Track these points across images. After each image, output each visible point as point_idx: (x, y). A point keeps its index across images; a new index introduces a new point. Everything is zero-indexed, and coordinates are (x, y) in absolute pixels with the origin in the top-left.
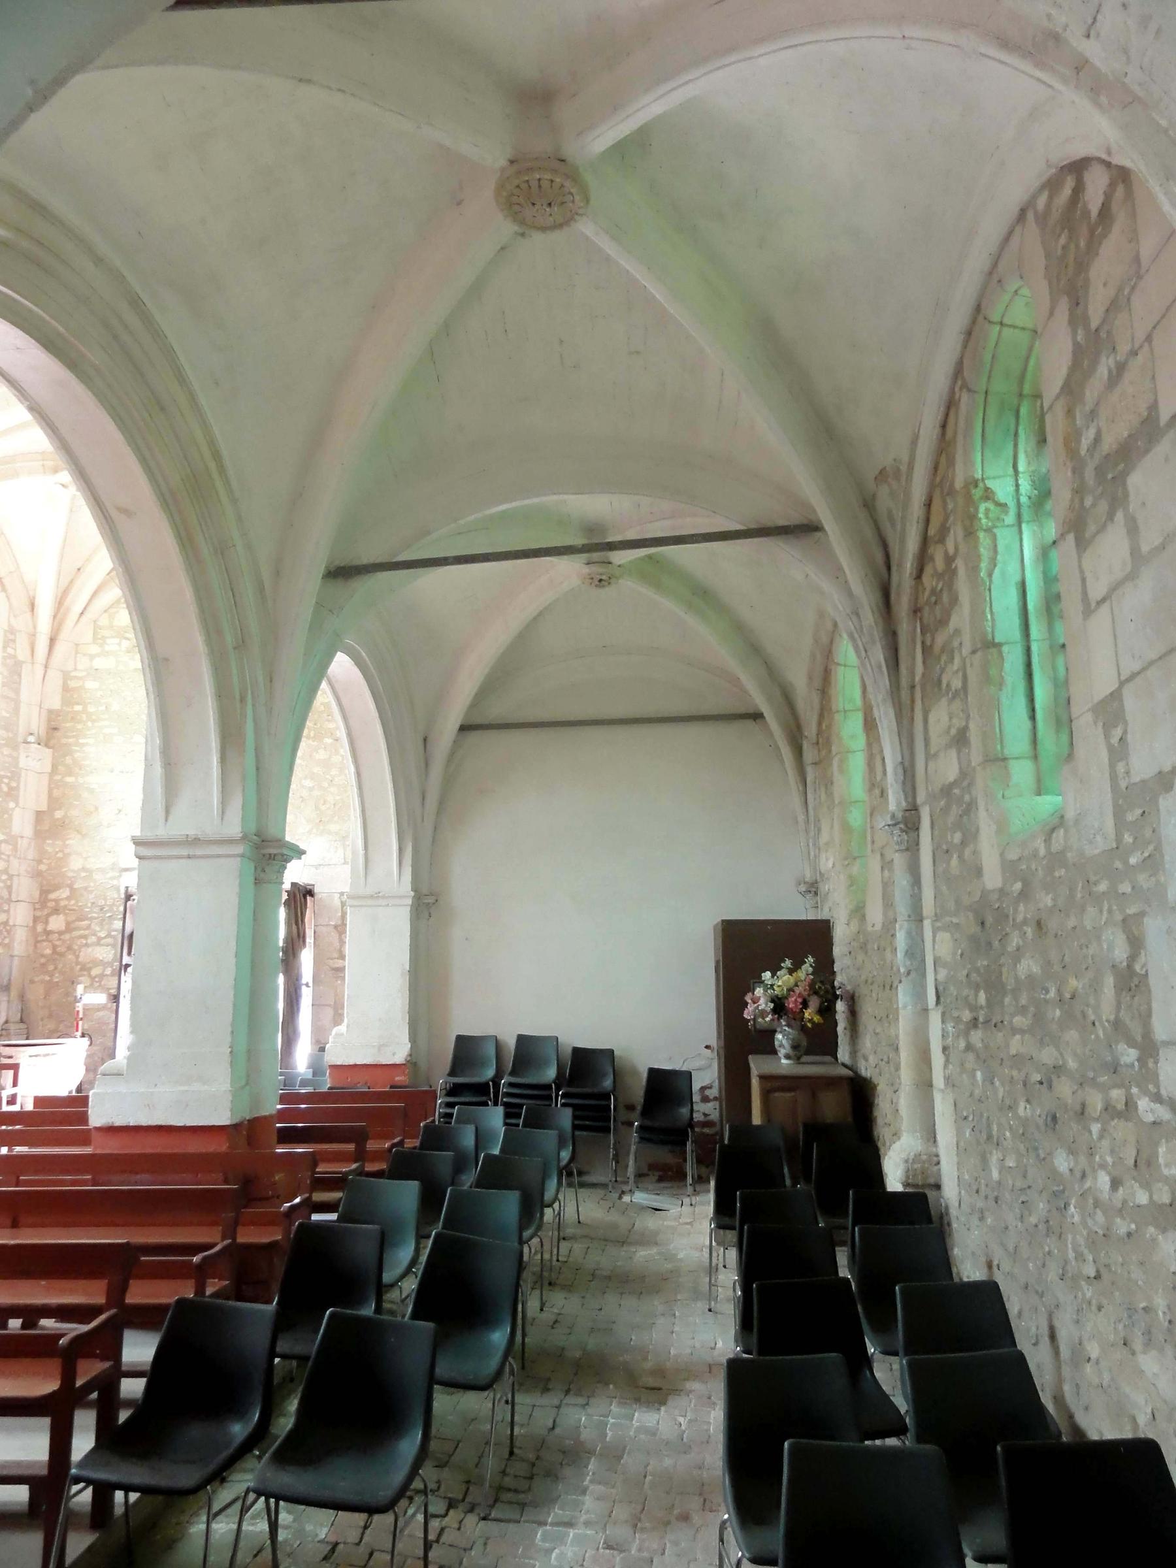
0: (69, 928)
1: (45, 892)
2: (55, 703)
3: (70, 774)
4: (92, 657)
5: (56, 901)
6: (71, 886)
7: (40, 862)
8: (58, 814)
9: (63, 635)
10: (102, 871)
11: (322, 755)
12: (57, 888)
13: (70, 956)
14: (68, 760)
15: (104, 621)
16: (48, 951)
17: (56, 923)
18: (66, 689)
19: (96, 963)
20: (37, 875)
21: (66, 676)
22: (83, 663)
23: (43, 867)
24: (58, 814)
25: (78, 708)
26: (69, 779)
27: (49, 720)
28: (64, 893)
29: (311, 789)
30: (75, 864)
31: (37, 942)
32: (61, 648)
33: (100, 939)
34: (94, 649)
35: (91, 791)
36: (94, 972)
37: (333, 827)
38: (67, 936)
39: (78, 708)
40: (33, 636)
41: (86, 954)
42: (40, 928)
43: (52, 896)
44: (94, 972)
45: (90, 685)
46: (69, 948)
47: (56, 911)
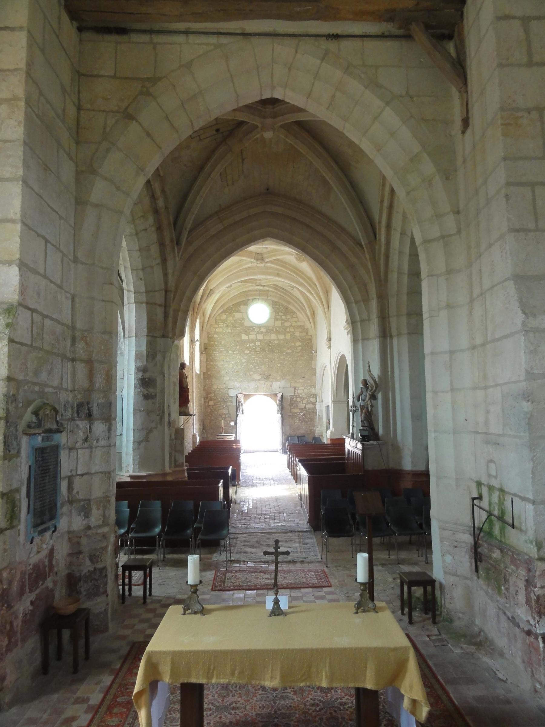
0: (215, 405)
1: (207, 394)
2: (206, 341)
3: (211, 361)
4: (216, 328)
5: (211, 397)
6: (214, 393)
7: (205, 386)
8: (209, 373)
9: (209, 322)
10: (223, 389)
11: (282, 357)
12: (211, 393)
13: (216, 412)
14: (211, 358)
15: (218, 318)
16: (209, 411)
17: (211, 403)
18: (208, 337)
19: (223, 414)
20: (204, 390)
21: (208, 333)
22: (213, 330)
23: (206, 388)
24: (209, 373)
25: (212, 343)
26: (212, 363)
27: (204, 346)
28: (213, 395)
29: (280, 367)
30: (215, 387)
31: (206, 408)
32: (209, 325)
33: (224, 408)
34: (216, 326)
35: (218, 367)
36: (223, 416)
37: (287, 377)
38: (214, 407)
39: (212, 343)
40: (203, 323)
41: (220, 412)
42: (206, 405)
43: (209, 396)
44: (223, 416)
45: (216, 336)
46: (215, 410)
47: (211, 400)
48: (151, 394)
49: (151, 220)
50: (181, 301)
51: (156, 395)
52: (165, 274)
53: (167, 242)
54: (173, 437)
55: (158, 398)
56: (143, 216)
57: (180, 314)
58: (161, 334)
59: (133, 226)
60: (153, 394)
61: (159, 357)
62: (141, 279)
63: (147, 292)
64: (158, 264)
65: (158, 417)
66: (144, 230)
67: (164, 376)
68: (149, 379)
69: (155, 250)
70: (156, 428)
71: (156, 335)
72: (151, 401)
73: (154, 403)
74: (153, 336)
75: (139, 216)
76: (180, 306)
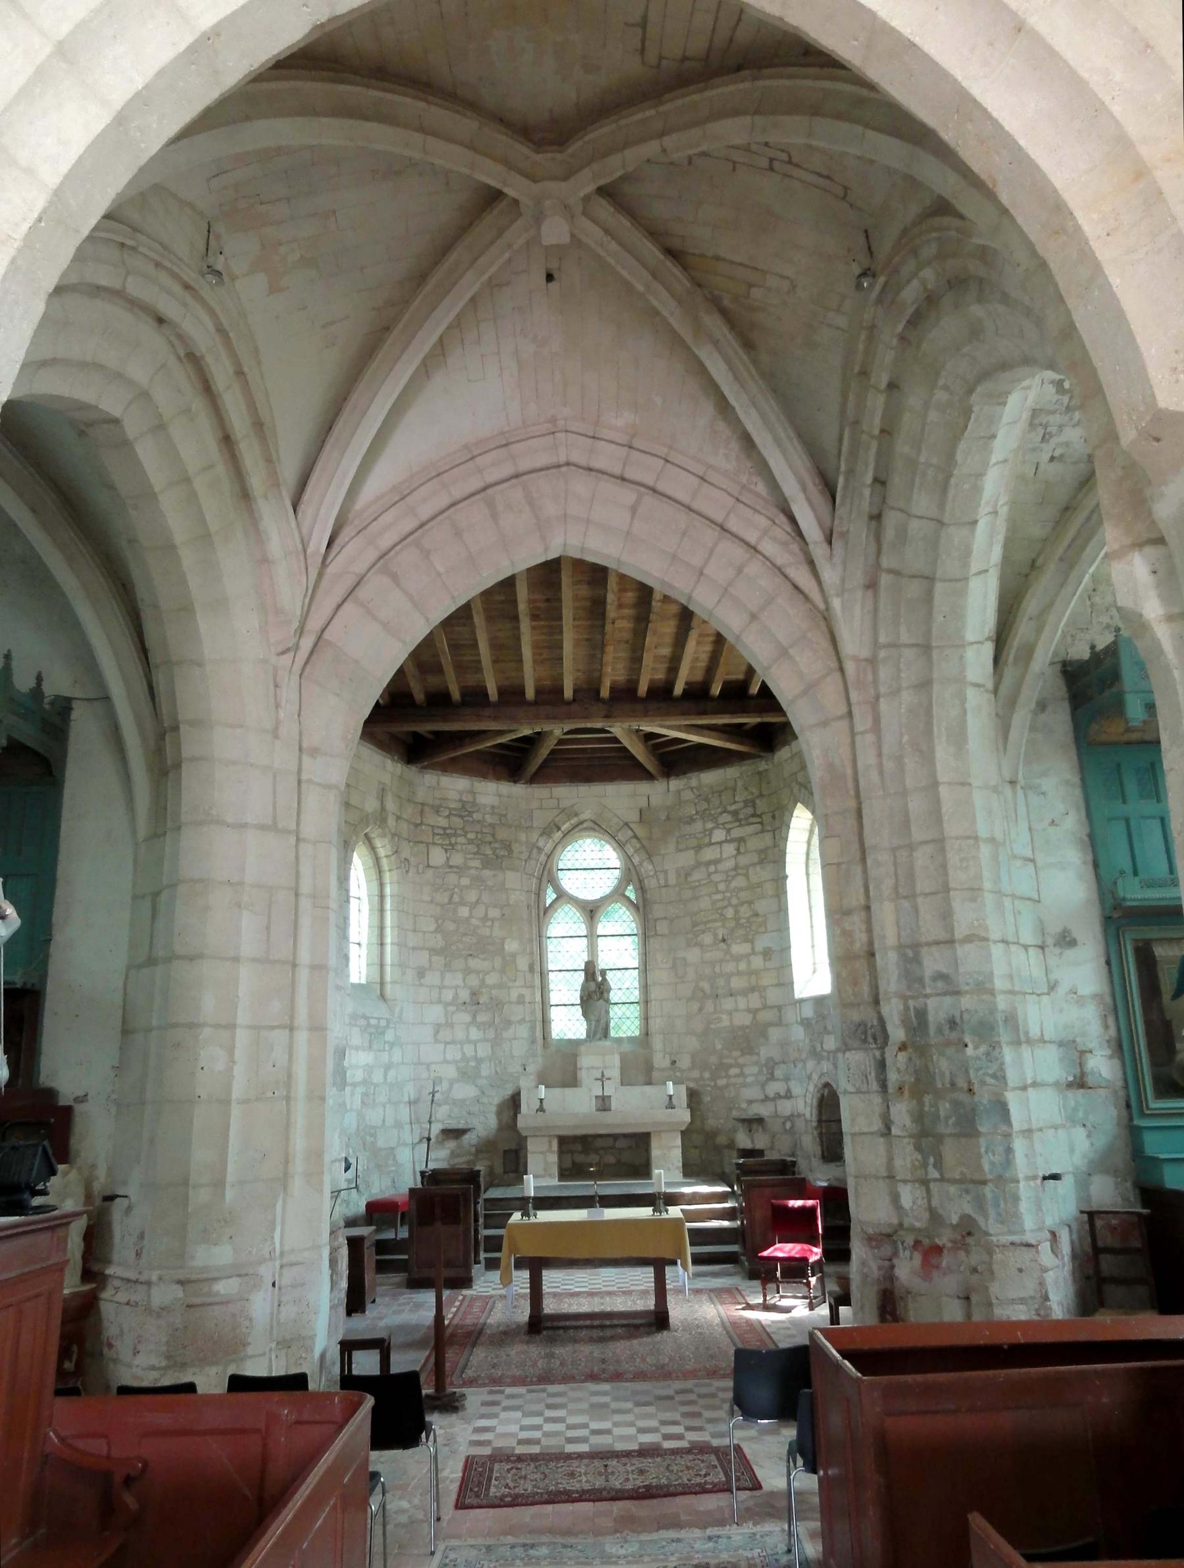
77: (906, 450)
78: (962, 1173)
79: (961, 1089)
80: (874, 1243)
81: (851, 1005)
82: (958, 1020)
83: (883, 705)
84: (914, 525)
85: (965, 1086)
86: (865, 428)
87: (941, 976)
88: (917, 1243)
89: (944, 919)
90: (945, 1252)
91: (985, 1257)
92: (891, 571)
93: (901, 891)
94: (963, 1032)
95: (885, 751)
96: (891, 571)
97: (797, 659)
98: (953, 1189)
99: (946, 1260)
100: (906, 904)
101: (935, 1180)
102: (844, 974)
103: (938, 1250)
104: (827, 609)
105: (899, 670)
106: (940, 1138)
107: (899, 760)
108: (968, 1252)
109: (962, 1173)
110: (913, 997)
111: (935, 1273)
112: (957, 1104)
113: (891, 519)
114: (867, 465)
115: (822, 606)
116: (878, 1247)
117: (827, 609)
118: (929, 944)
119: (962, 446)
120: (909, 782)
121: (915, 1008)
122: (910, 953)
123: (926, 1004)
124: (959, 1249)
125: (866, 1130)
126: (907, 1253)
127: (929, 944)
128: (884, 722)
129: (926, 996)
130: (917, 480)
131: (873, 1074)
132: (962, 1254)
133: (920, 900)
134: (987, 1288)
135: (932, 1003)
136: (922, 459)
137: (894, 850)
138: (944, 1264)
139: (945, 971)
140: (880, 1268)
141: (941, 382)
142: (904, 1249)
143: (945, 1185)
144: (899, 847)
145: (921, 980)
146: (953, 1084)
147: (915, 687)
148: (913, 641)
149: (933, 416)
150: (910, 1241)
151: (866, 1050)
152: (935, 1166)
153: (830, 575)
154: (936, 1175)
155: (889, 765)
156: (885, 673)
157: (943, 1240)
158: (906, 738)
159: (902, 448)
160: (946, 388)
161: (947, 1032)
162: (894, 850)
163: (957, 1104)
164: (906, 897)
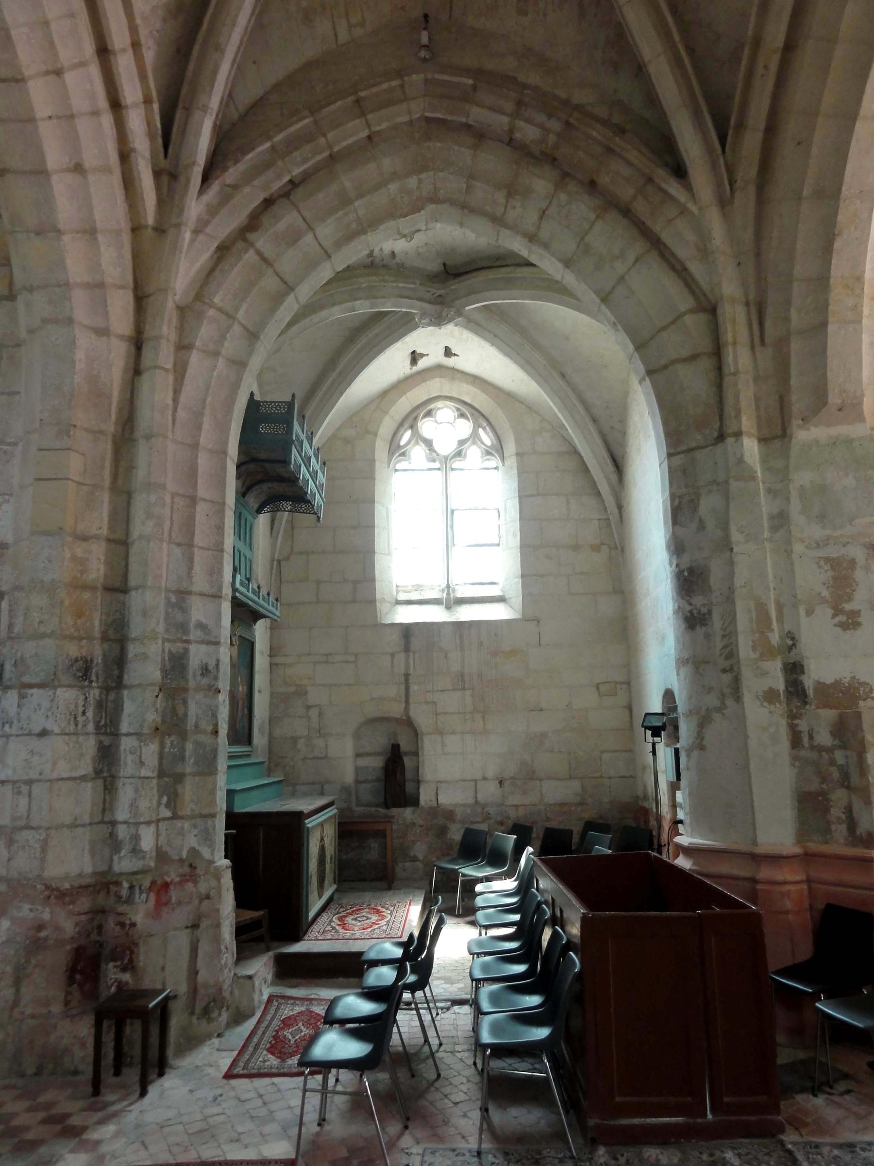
48: (699, 612)
49: (540, 184)
50: (788, 303)
51: (710, 612)
52: (680, 271)
53: (626, 193)
54: (824, 738)
55: (717, 622)
56: (509, 195)
57: (796, 346)
58: (716, 434)
59: (507, 232)
60: (704, 610)
61: (708, 504)
62: (614, 323)
63: (640, 347)
64: (637, 260)
65: (727, 678)
66: (541, 218)
67: (732, 550)
68: (691, 570)
69: (608, 236)
70: (720, 709)
71: (694, 444)
72: (700, 631)
73: (707, 636)
74: (691, 450)
75: (503, 201)
76: (787, 319)
77: (348, 184)
78: (192, 810)
79: (204, 732)
80: (67, 899)
81: (71, 638)
82: (210, 668)
83: (195, 358)
84: (309, 238)
85: (210, 728)
86: (330, 136)
87: (201, 626)
88: (153, 883)
89: (211, 575)
90: (172, 887)
91: (213, 883)
92: (259, 253)
93: (174, 536)
94: (216, 678)
95: (183, 398)
96: (259, 253)
97: (102, 249)
98: (187, 825)
99: (174, 894)
100: (178, 551)
101: (164, 819)
102: (67, 603)
103: (166, 886)
104: (160, 230)
105: (223, 337)
106: (179, 778)
107: (198, 415)
108: (195, 883)
109: (192, 810)
110: (169, 640)
111: (165, 909)
112: (197, 744)
113: (287, 219)
114: (305, 161)
115: (150, 219)
116: (72, 902)
117: (160, 230)
118: (196, 594)
119: (391, 224)
120: (202, 441)
121: (170, 651)
122: (173, 599)
123: (186, 651)
124: (188, 881)
125: (65, 775)
126: (144, 896)
127: (196, 594)
128: (190, 372)
129: (188, 642)
130: (341, 213)
131: (90, 714)
132: (190, 886)
133: (196, 551)
134: (218, 910)
135: (193, 648)
136: (357, 204)
137: (173, 495)
138: (174, 899)
139: (204, 621)
140: (77, 924)
141: (423, 176)
142: (141, 893)
143: (178, 823)
144: (178, 494)
145: (183, 627)
146: (197, 726)
147: (227, 359)
148: (244, 322)
149: (393, 187)
150: (147, 883)
151: (82, 688)
152: (168, 806)
153: (194, 207)
154: (168, 814)
155: (181, 414)
156: (205, 332)
157: (172, 874)
158: (209, 399)
159: (347, 181)
160: (420, 181)
161: (199, 678)
162: (173, 495)
163: (197, 744)
164: (179, 545)
